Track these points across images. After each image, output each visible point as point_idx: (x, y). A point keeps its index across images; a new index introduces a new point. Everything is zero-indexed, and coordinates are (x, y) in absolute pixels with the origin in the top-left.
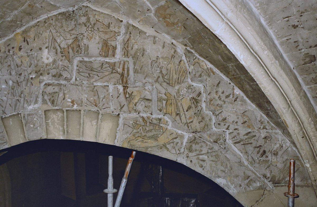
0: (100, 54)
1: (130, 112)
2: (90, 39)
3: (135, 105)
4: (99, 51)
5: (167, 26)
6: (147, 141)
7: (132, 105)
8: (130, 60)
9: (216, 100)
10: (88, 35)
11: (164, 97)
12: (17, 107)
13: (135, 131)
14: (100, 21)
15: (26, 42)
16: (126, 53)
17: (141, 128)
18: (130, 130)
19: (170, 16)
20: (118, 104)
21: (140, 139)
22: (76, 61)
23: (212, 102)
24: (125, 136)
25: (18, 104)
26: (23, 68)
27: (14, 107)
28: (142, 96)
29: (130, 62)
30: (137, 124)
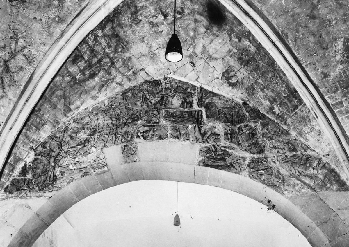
0: (181, 107)
1: (204, 142)
2: (173, 97)
3: (208, 138)
4: (180, 104)
5: (230, 86)
6: (218, 161)
7: (205, 138)
8: (203, 110)
9: (267, 134)
10: (172, 95)
11: (229, 132)
12: (116, 142)
13: (208, 155)
14: (181, 86)
15: (125, 99)
16: (200, 105)
17: (213, 153)
18: (204, 154)
19: (232, 78)
20: (195, 138)
21: (212, 160)
22: (163, 112)
23: (264, 136)
24: (201, 158)
25: (117, 139)
26: (122, 116)
27: (113, 141)
28: (213, 132)
29: (203, 111)
30: (210, 150)
